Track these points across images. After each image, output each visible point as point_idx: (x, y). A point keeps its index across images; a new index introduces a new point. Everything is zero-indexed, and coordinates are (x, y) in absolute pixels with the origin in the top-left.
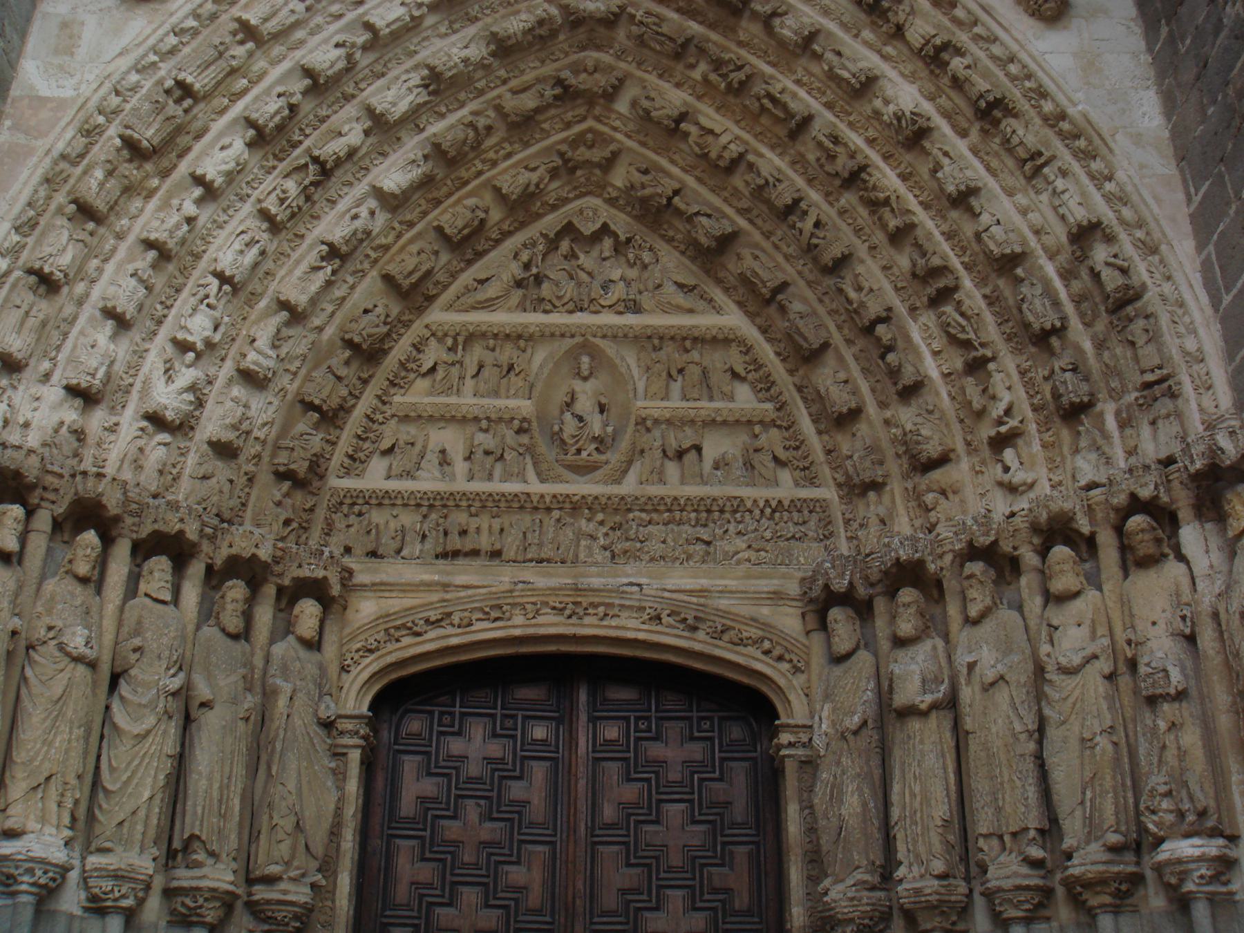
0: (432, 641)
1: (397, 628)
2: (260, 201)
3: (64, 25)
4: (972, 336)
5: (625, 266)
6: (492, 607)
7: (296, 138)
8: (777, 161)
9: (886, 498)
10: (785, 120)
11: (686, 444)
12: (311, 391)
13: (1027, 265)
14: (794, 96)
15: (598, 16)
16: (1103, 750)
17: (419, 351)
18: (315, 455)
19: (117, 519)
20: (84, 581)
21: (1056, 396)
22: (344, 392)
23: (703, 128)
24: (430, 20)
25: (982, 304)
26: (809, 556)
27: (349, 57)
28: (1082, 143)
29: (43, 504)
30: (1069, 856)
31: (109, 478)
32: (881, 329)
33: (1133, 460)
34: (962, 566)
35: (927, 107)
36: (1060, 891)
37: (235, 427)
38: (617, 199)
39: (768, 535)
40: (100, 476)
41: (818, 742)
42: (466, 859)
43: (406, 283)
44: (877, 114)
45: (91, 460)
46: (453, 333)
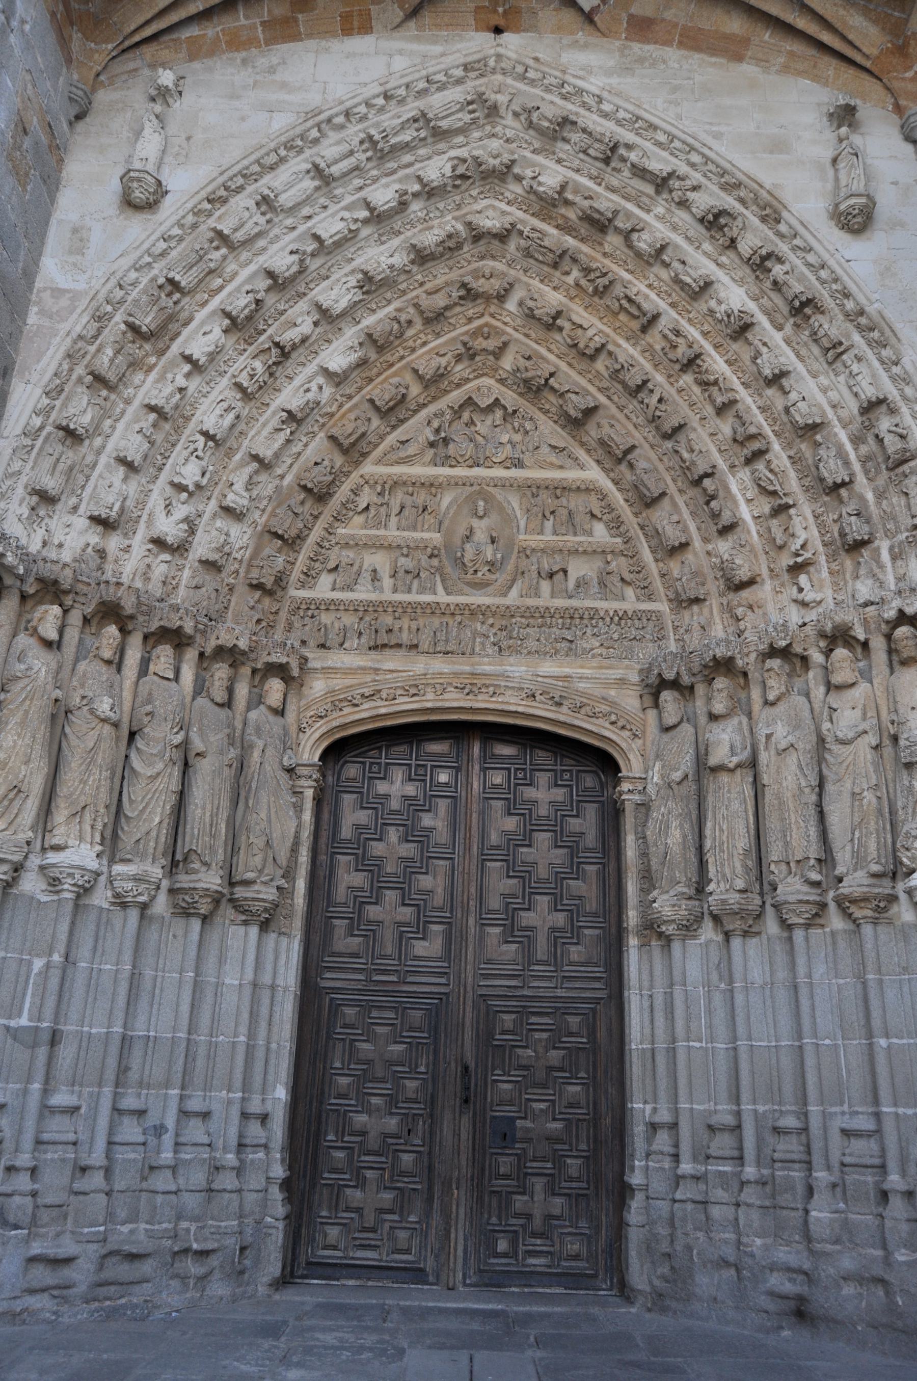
0: (366, 710)
1: (341, 701)
2: (234, 376)
3: (75, 231)
4: (778, 488)
5: (511, 432)
6: (410, 686)
7: (261, 327)
8: (631, 350)
9: (706, 611)
10: (638, 317)
13: (825, 433)
14: (647, 297)
15: (494, 231)
16: (870, 803)
19: (132, 617)
20: (109, 662)
21: (842, 534)
22: (301, 525)
23: (574, 324)
24: (365, 232)
25: (787, 463)
26: (646, 652)
27: (302, 261)
28: (876, 335)
29: (76, 605)
30: (840, 880)
31: (126, 586)
32: (707, 482)
33: (901, 584)
34: (763, 662)
35: (752, 306)
36: (832, 906)
37: (219, 550)
38: (506, 379)
39: (616, 636)
40: (119, 584)
41: (651, 790)
42: (389, 870)
44: (712, 312)
45: (110, 573)
46: (380, 482)
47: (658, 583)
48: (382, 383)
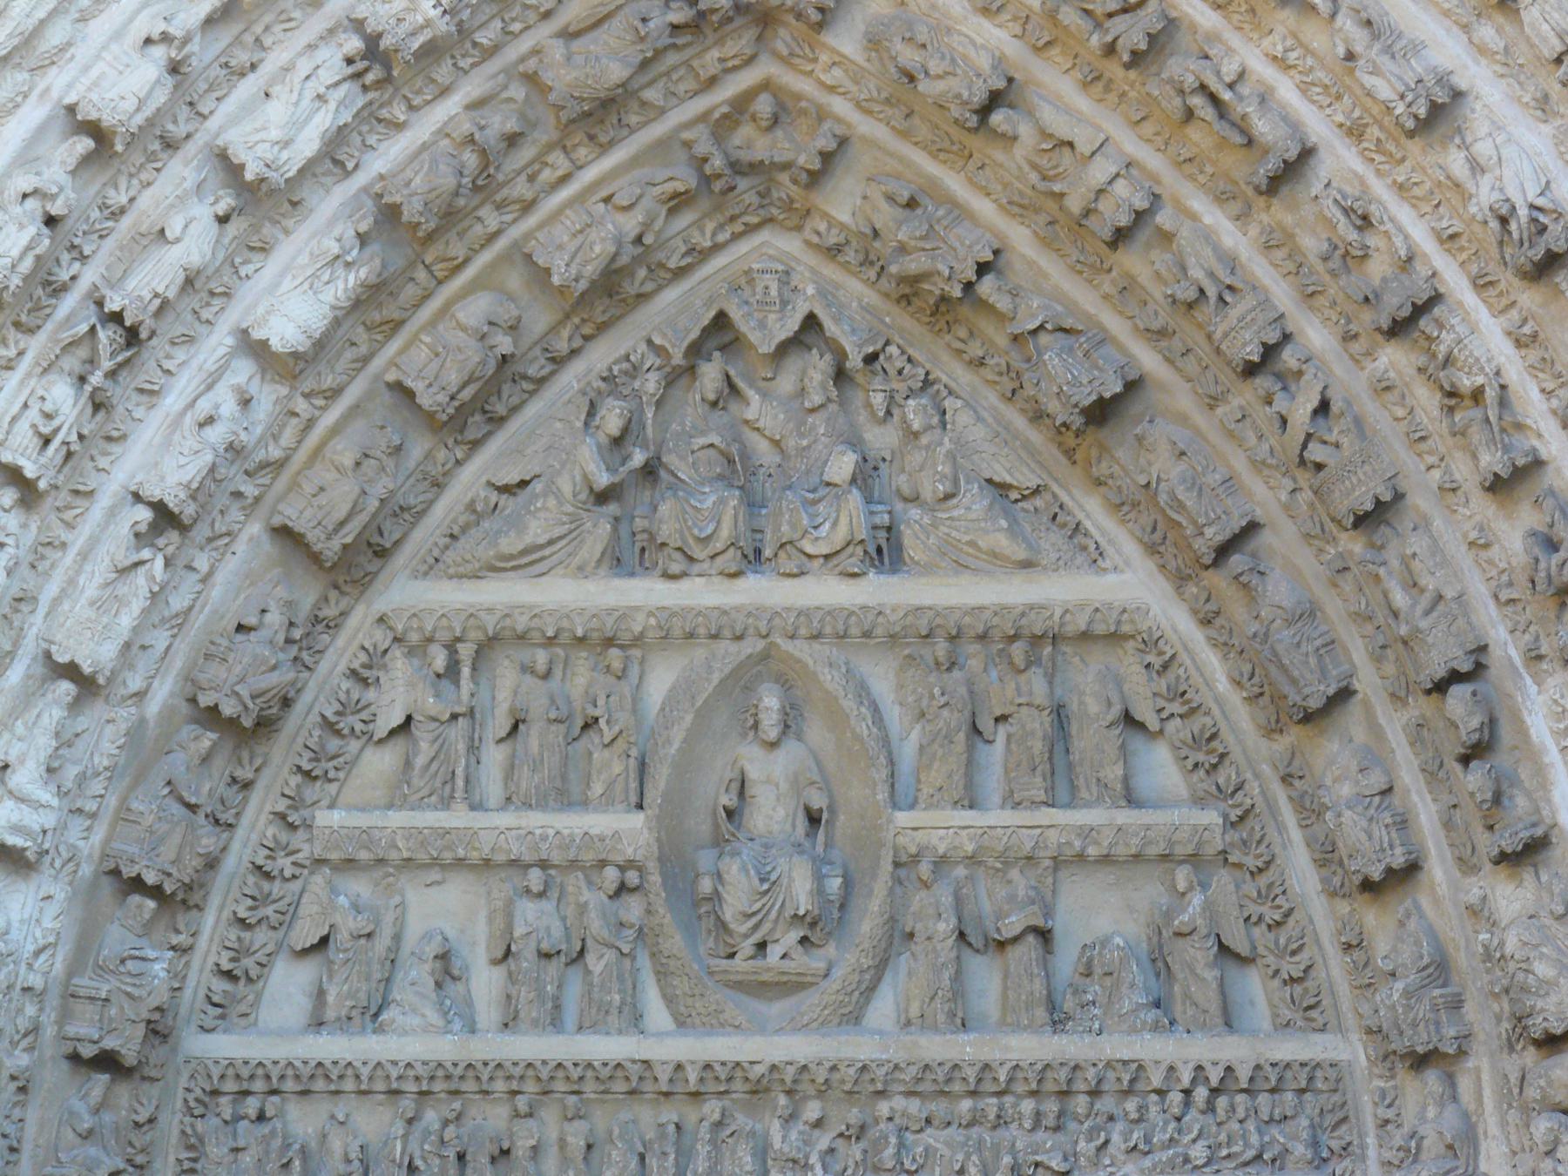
8: (1231, 236)
11: (1014, 923)
12: (133, 849)
14: (1265, 98)
17: (365, 682)
18: (158, 1009)
23: (1045, 135)
39: (1199, 1153)
43: (331, 549)
46: (443, 636)
47: (1335, 969)
48: (432, 323)
